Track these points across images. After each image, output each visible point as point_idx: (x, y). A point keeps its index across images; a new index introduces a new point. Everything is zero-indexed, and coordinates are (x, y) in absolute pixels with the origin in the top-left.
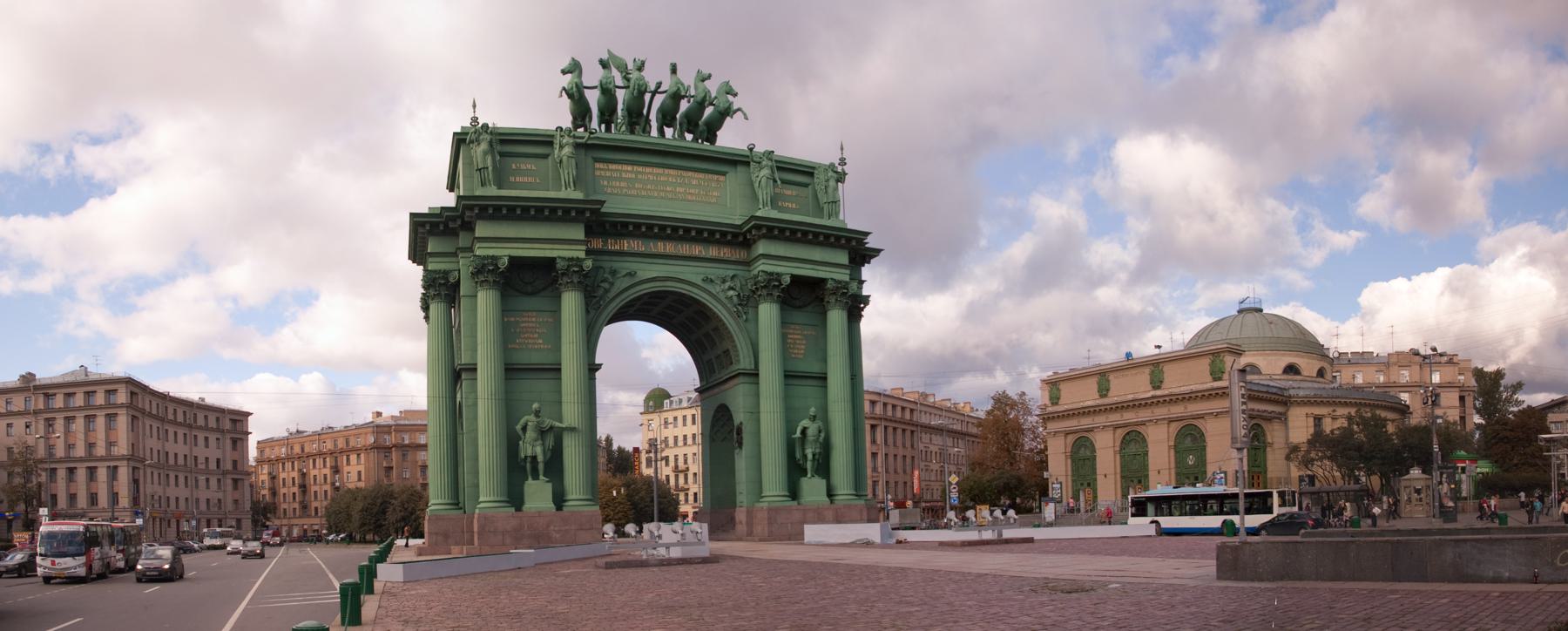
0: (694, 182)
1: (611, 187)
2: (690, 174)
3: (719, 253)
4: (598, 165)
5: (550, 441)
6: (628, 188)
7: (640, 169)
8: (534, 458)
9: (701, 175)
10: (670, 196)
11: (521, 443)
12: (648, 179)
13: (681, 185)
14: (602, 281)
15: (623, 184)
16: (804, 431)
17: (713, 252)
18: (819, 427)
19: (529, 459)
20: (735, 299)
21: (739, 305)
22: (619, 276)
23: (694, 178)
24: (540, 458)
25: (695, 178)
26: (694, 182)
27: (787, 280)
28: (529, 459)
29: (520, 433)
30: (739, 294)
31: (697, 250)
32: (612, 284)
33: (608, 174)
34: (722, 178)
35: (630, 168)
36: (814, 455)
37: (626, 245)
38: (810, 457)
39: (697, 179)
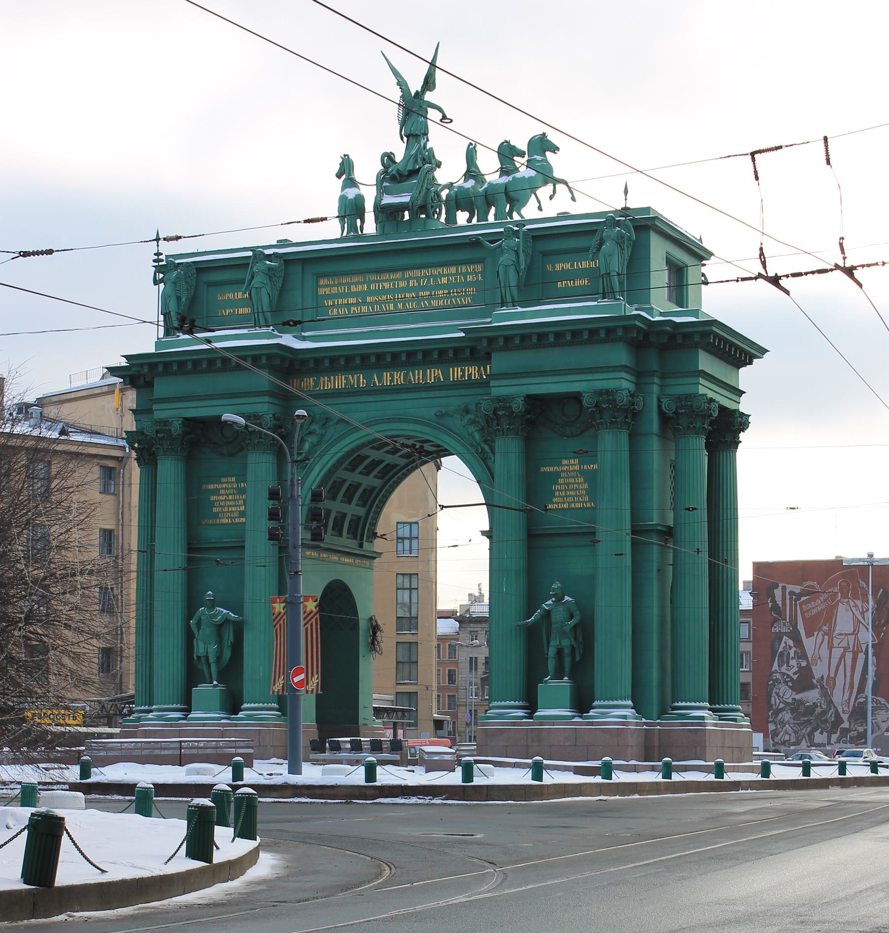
0: (444, 280)
1: (338, 306)
2: (435, 271)
3: (463, 376)
4: (322, 282)
5: (229, 636)
6: (357, 304)
7: (374, 277)
8: (207, 658)
9: (453, 270)
10: (409, 306)
11: (195, 640)
12: (383, 286)
13: (424, 289)
14: (310, 433)
15: (352, 300)
16: (547, 614)
17: (456, 373)
18: (569, 609)
19: (203, 660)
20: (477, 436)
21: (485, 442)
22: (331, 423)
23: (441, 276)
24: (212, 659)
25: (447, 275)
26: (444, 280)
27: (518, 405)
28: (203, 660)
29: (194, 628)
30: (483, 428)
31: (433, 374)
32: (323, 435)
33: (335, 290)
34: (479, 268)
35: (360, 278)
36: (560, 652)
37: (343, 381)
38: (552, 652)
39: (444, 276)
